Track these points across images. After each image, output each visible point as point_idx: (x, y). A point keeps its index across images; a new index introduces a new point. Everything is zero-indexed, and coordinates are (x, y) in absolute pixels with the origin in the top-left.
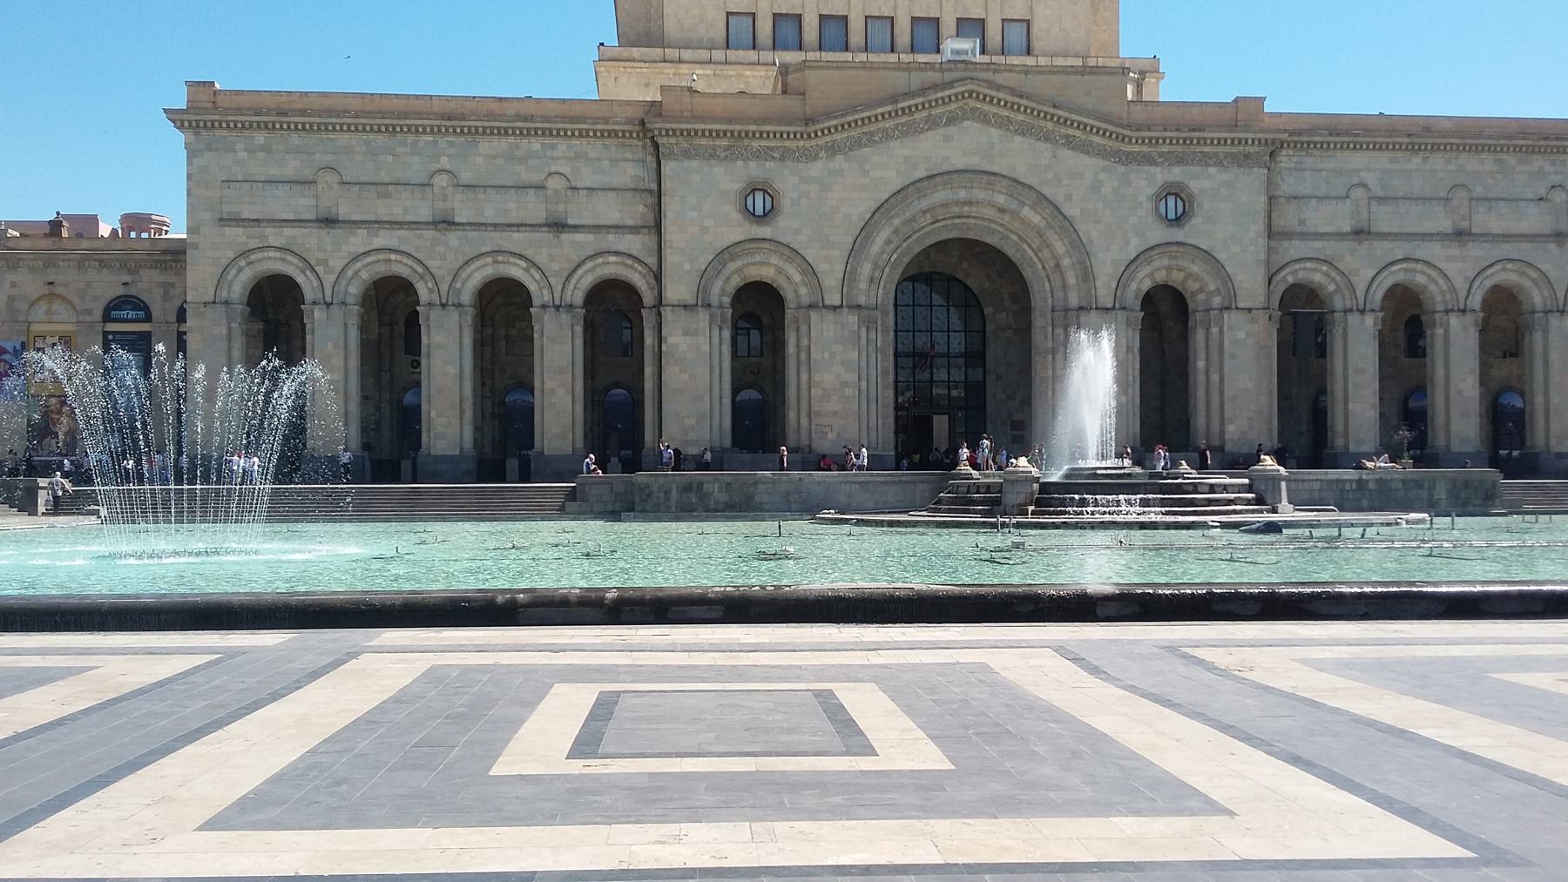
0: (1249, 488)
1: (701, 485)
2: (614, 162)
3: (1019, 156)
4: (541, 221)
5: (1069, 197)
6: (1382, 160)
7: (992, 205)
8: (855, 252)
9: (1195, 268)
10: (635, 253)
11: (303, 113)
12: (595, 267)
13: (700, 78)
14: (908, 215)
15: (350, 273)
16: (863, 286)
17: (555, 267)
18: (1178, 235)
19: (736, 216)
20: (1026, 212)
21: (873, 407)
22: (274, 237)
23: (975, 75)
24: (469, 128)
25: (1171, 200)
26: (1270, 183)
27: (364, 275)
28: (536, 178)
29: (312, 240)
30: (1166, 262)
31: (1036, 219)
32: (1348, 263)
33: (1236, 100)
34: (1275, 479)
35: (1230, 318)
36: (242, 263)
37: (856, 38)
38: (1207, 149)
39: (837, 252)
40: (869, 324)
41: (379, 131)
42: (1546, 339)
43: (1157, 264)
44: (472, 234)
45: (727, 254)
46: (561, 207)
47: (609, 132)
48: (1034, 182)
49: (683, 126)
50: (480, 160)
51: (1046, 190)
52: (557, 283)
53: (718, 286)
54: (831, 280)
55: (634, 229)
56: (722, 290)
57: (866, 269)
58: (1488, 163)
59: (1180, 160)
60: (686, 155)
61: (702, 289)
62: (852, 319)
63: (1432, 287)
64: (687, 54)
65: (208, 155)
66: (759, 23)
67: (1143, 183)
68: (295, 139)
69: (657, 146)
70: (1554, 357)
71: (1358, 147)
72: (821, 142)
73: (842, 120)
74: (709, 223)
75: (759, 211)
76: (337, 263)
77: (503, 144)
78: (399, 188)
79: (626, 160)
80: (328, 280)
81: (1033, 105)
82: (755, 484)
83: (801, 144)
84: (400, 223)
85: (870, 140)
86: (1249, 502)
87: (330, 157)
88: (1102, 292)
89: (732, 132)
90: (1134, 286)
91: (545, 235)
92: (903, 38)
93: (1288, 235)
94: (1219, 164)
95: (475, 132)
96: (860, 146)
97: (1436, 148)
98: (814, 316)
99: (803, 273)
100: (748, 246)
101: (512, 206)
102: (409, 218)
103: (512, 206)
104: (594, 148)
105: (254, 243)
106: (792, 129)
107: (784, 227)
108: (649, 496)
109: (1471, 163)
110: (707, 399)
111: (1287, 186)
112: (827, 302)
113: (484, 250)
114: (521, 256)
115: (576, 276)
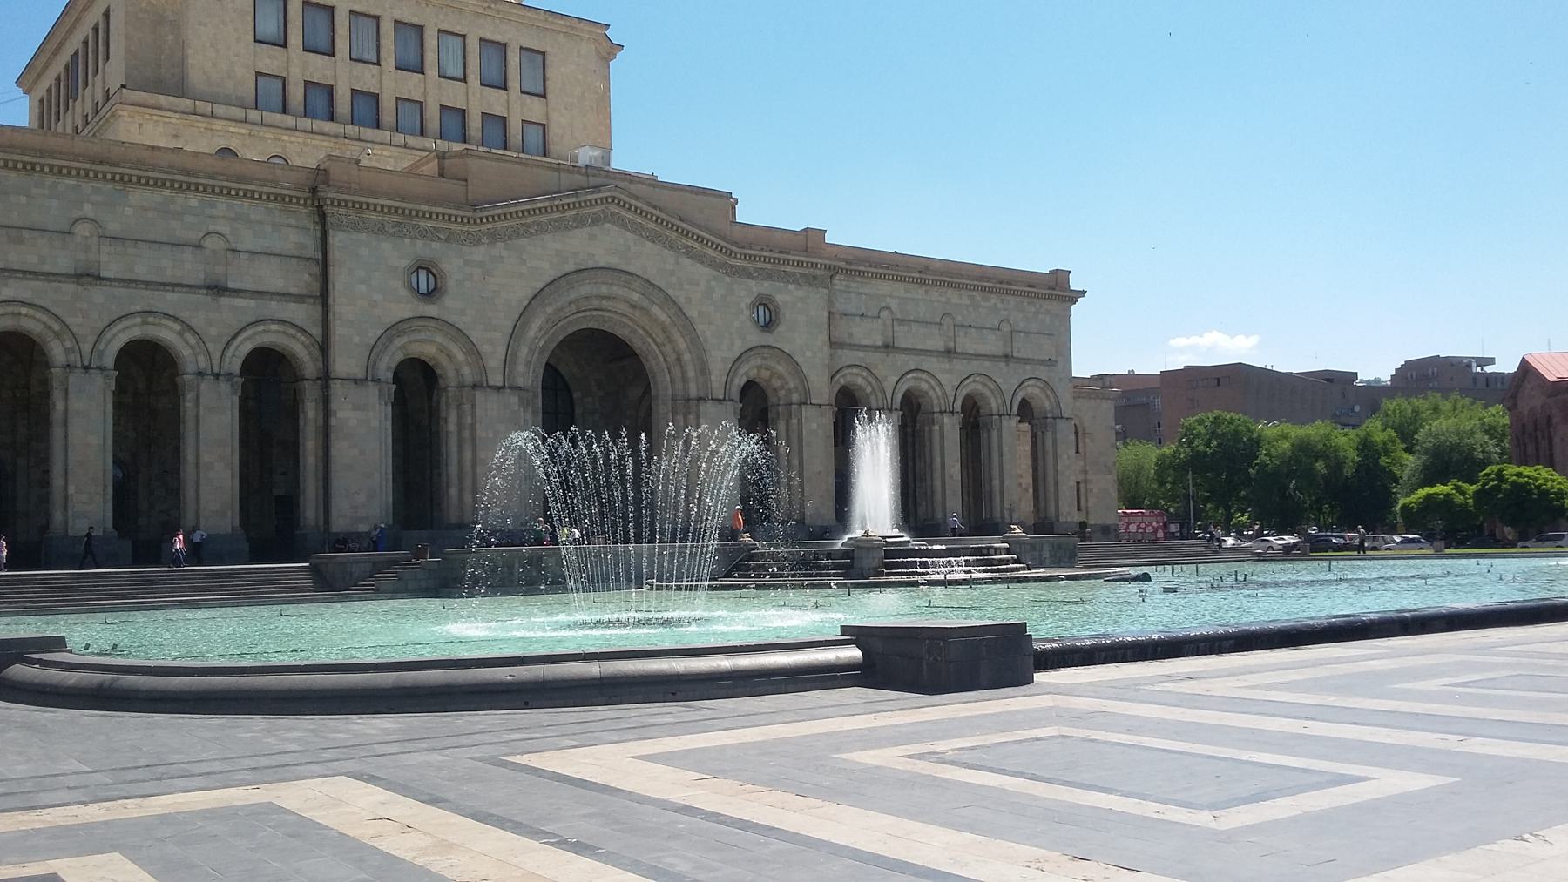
0: (1008, 551)
3: (649, 259)
4: (202, 283)
5: (689, 300)
6: (900, 289)
7: (626, 301)
8: (514, 336)
9: (780, 369)
13: (233, 135)
17: (213, 331)
18: (768, 339)
19: (403, 292)
20: (655, 310)
23: (621, 184)
24: (122, 175)
25: (761, 308)
26: (830, 303)
28: (193, 236)
30: (759, 362)
31: (663, 317)
32: (880, 371)
33: (806, 230)
35: (807, 412)
37: (388, 117)
38: (789, 269)
39: (498, 335)
40: (524, 404)
41: (15, 168)
42: (1000, 437)
43: (752, 363)
44: (120, 291)
45: (396, 329)
46: (220, 269)
47: (276, 196)
48: (663, 286)
49: (356, 199)
50: (129, 211)
51: (671, 292)
54: (494, 362)
55: (299, 299)
56: (387, 364)
57: (523, 352)
59: (769, 276)
60: (355, 227)
61: (371, 364)
62: (514, 400)
63: (931, 393)
64: (220, 110)
66: (291, 88)
67: (743, 293)
69: (322, 217)
70: (1005, 449)
71: (886, 278)
72: (483, 228)
74: (377, 297)
77: (157, 196)
78: (36, 234)
81: (663, 216)
83: (466, 228)
84: (35, 273)
88: (715, 385)
90: (737, 381)
91: (203, 298)
92: (433, 123)
93: (842, 345)
94: (796, 282)
95: (126, 181)
96: (518, 236)
97: (935, 283)
98: (479, 395)
100: (416, 323)
102: (46, 268)
104: (256, 211)
106: (461, 213)
107: (451, 306)
109: (954, 297)
111: (840, 306)
113: (133, 309)
114: (176, 319)
115: (235, 343)
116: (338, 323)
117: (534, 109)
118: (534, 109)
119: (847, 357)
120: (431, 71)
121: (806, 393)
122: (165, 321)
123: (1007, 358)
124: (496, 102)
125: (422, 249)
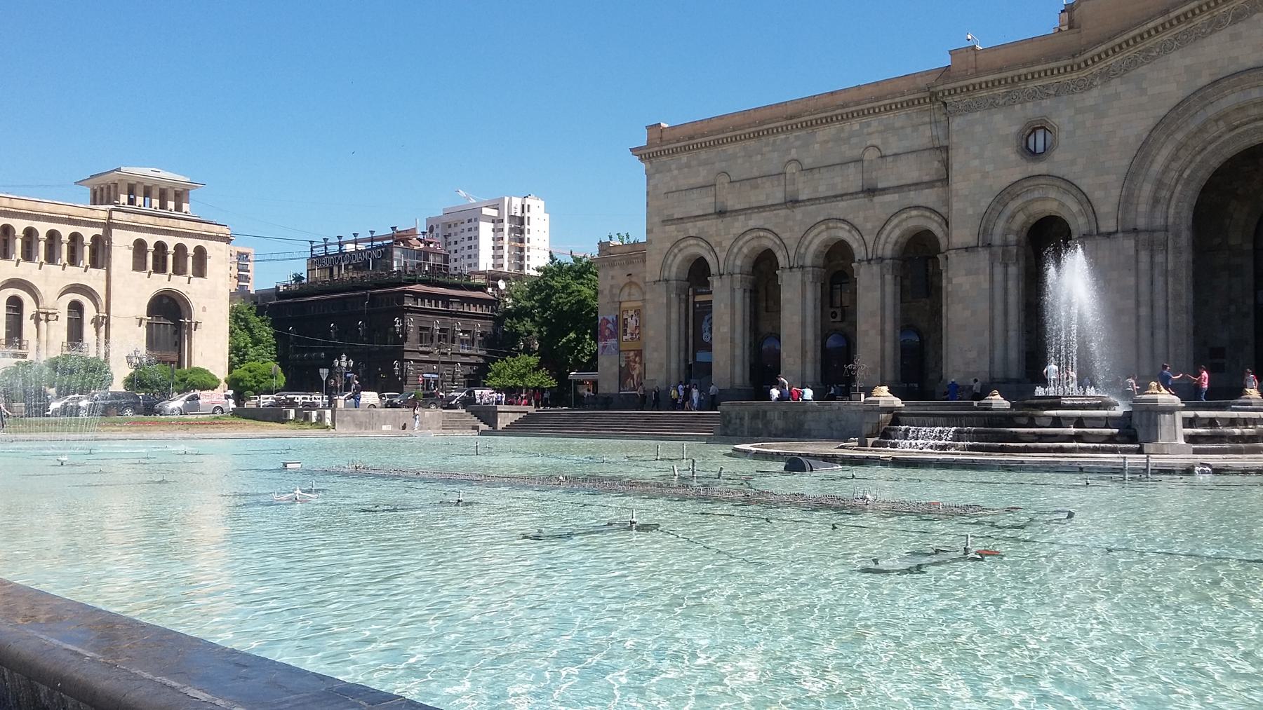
1: (765, 412)
2: (915, 127)
8: (1131, 177)
10: (930, 205)
11: (703, 135)
12: (901, 222)
14: (1192, 127)
15: (735, 250)
16: (1143, 208)
17: (869, 226)
19: (1014, 157)
21: (1160, 335)
22: (692, 229)
27: (745, 250)
28: (856, 153)
29: (711, 228)
34: (1153, 412)
36: (676, 251)
50: (817, 146)
52: (869, 239)
53: (1000, 225)
54: (1107, 204)
55: (930, 184)
60: (969, 109)
62: (1129, 244)
65: (657, 176)
68: (703, 155)
69: (945, 104)
72: (1095, 69)
73: (1111, 44)
74: (989, 168)
75: (1040, 148)
76: (727, 244)
79: (924, 124)
80: (722, 256)
82: (805, 412)
83: (1074, 76)
85: (1147, 57)
86: (1111, 438)
87: (724, 164)
89: (1006, 79)
91: (862, 201)
95: (810, 125)
99: (1080, 203)
100: (1026, 184)
101: (838, 180)
102: (770, 202)
103: (838, 180)
104: (898, 119)
107: (1060, 162)
108: (730, 422)
110: (987, 334)
112: (1103, 229)
114: (844, 221)
116: (955, 199)
122: (840, 225)
125: (1030, 111)
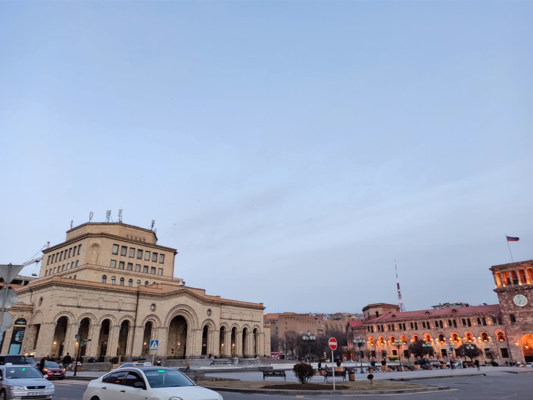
18: (209, 318)
19: (149, 310)
20: (190, 312)
22: (67, 309)
29: (74, 310)
35: (216, 332)
40: (167, 331)
52: (118, 321)
54: (163, 323)
55: (132, 311)
58: (244, 309)
61: (143, 323)
76: (79, 315)
104: (128, 296)
105: (63, 310)
109: (243, 309)
117: (161, 266)
118: (161, 266)
119: (223, 321)
120: (143, 259)
121: (215, 328)
123: (252, 321)
124: (154, 265)
